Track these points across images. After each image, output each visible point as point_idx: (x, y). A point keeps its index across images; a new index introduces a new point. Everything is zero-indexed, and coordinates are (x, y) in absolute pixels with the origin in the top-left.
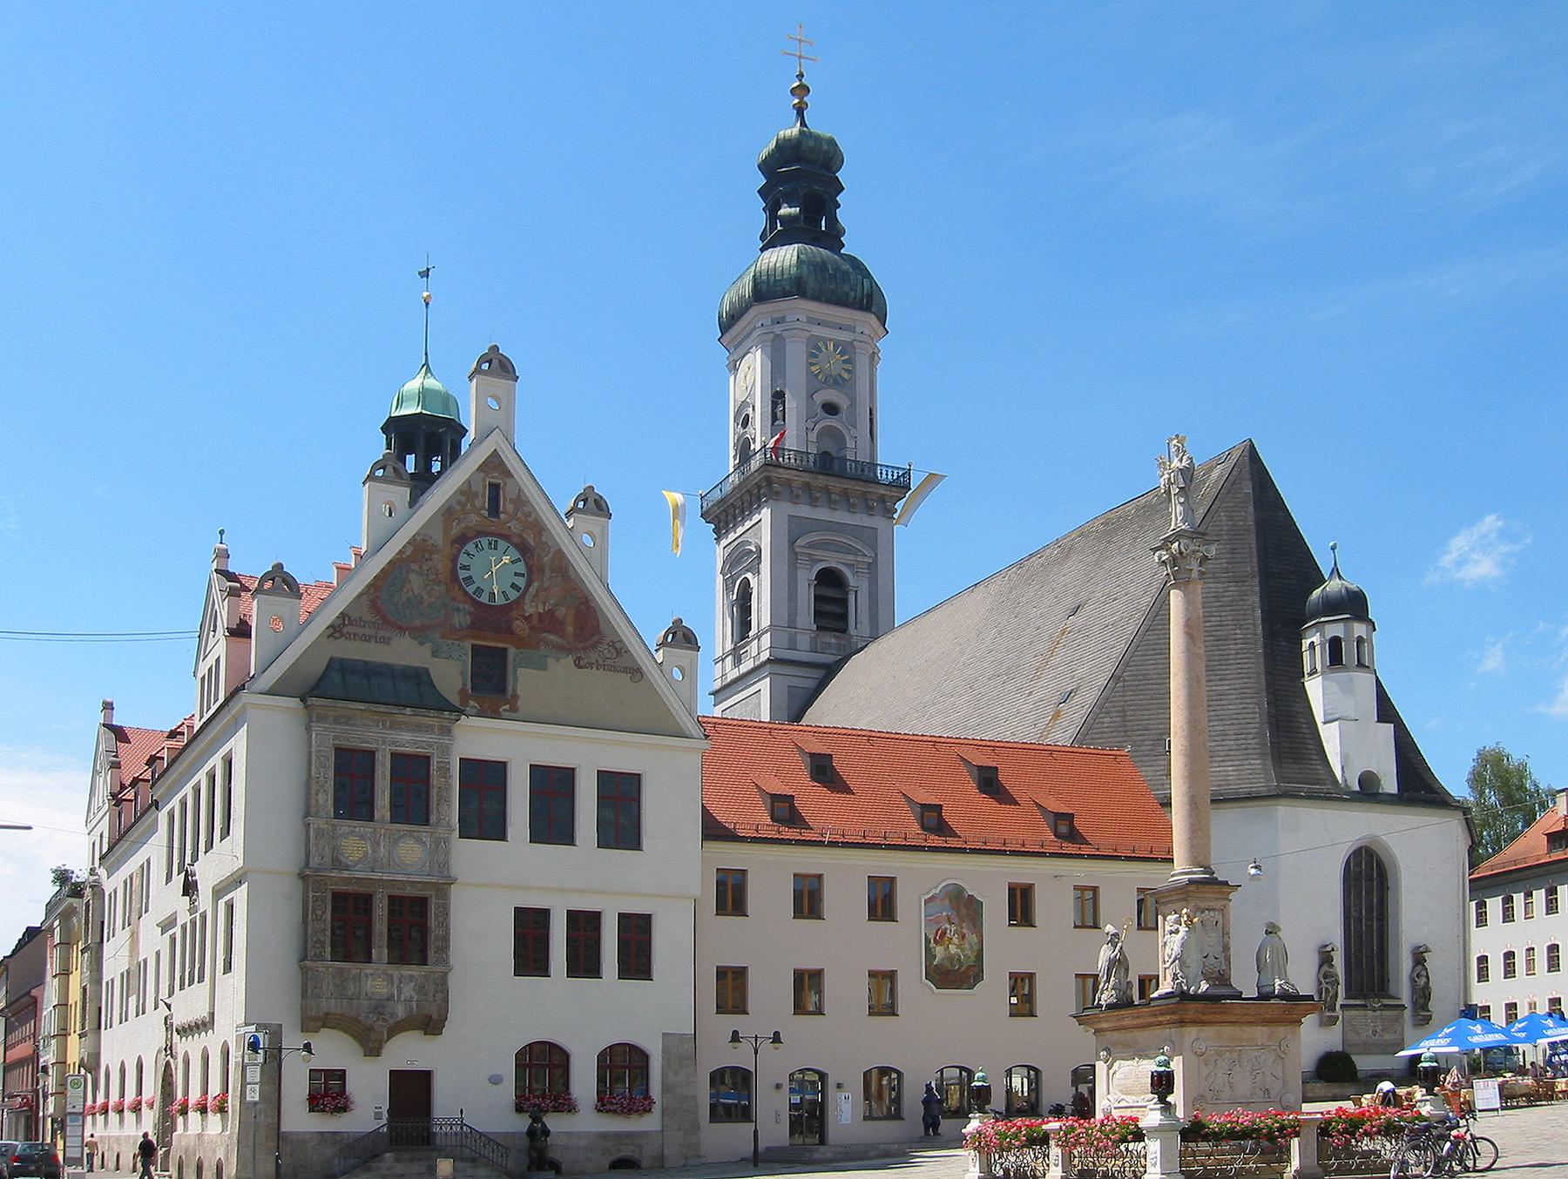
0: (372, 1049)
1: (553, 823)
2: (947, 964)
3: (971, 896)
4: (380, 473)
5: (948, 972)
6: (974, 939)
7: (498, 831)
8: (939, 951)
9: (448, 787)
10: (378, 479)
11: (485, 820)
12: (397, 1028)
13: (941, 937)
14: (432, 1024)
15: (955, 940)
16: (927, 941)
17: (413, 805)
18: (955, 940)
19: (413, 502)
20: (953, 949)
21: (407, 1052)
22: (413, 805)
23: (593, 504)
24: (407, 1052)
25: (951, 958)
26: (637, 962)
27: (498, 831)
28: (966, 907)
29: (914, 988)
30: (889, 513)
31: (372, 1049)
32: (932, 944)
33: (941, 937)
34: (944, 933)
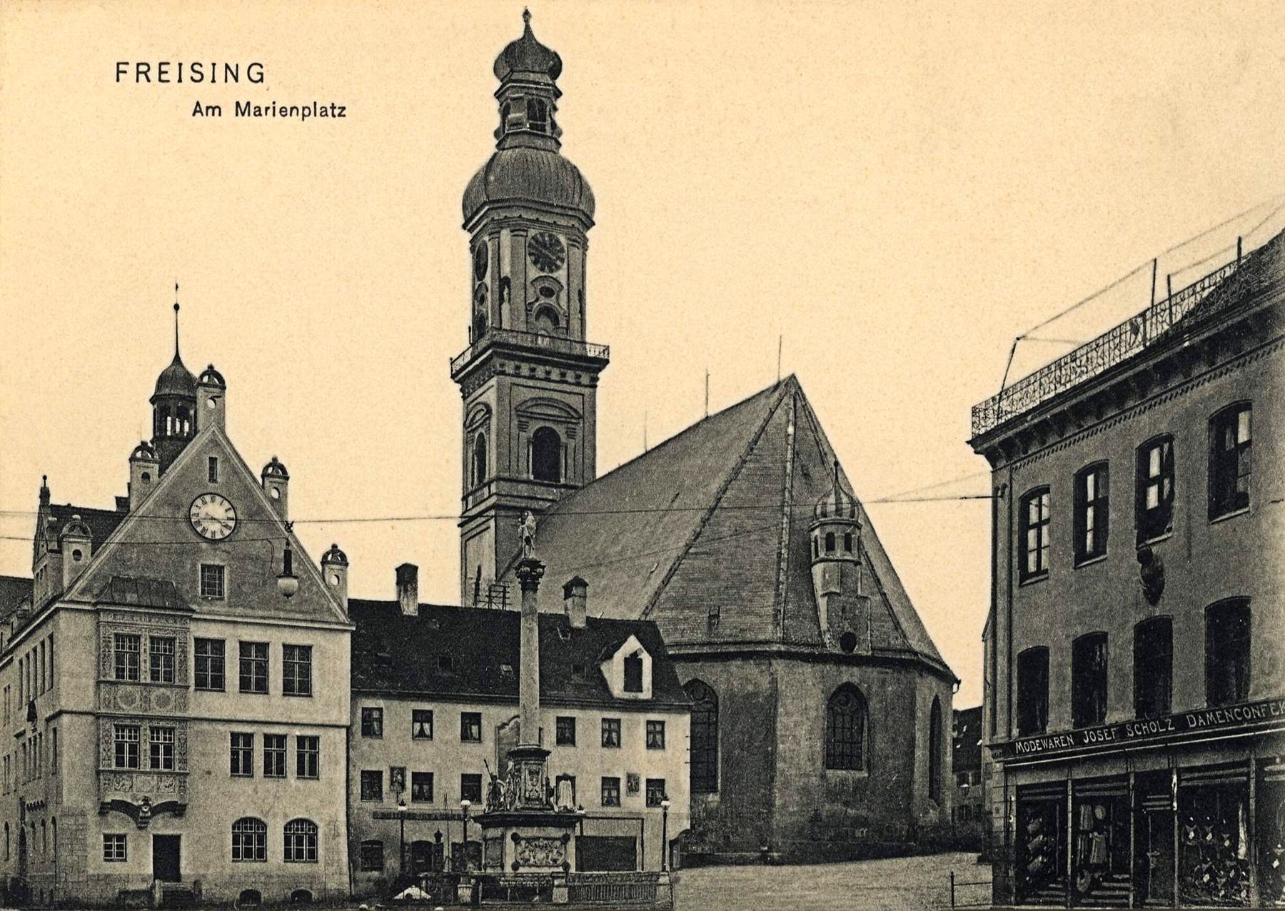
0: (142, 825)
1: (254, 682)
4: (139, 454)
7: (218, 684)
9: (184, 661)
10: (139, 460)
11: (212, 680)
12: (156, 811)
14: (177, 810)
17: (165, 672)
19: (162, 471)
21: (163, 826)
22: (165, 672)
23: (276, 471)
24: (163, 826)
26: (309, 768)
27: (218, 684)
31: (142, 825)
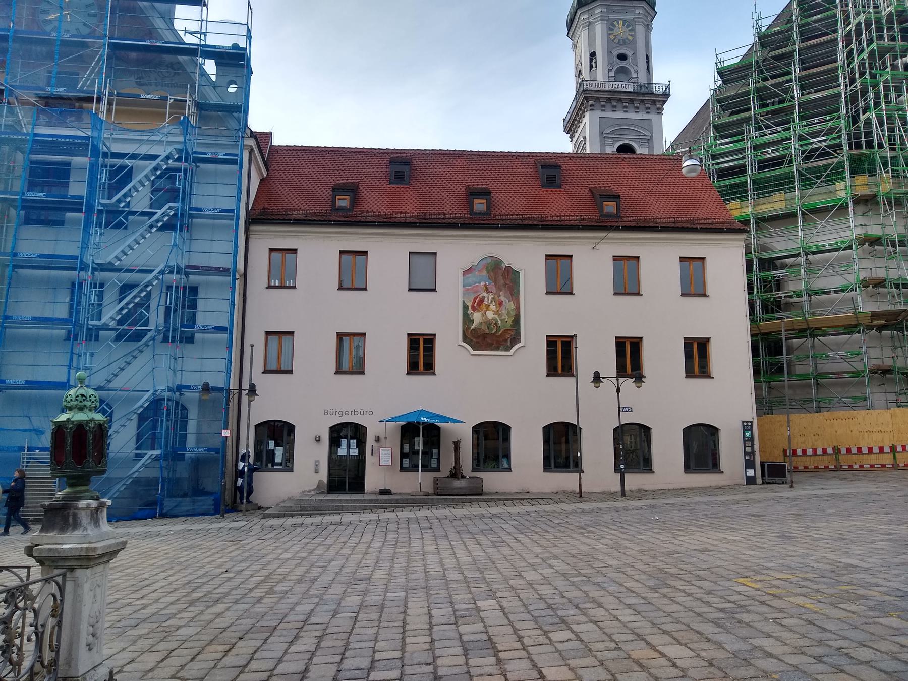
2: (484, 328)
3: (509, 269)
5: (484, 336)
6: (512, 306)
8: (477, 317)
13: (479, 304)
15: (493, 307)
16: (465, 307)
18: (493, 307)
20: (490, 315)
25: (488, 323)
28: (505, 278)
29: (450, 349)
30: (660, 111)
32: (470, 311)
33: (479, 304)
34: (482, 301)
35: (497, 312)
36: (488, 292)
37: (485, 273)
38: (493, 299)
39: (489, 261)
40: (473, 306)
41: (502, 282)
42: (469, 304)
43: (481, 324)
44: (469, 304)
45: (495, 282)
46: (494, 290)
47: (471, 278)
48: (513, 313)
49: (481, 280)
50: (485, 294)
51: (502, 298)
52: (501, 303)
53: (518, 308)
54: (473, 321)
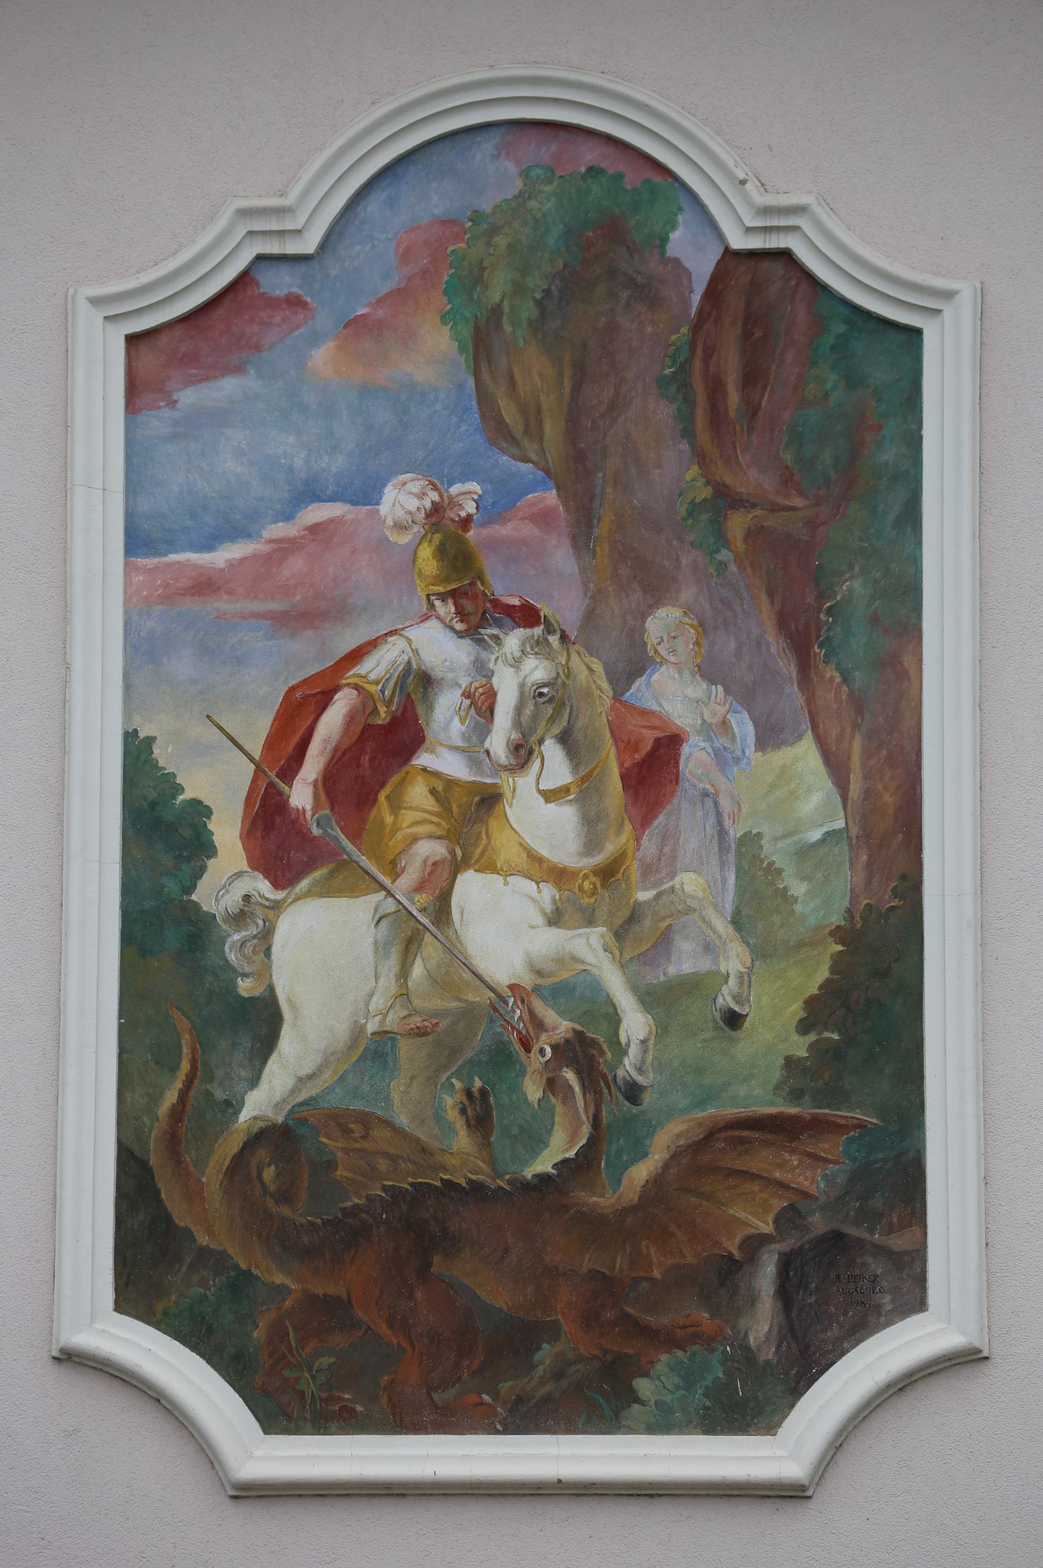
2: (420, 1107)
3: (764, 284)
6: (797, 793)
8: (322, 962)
13: (350, 779)
15: (541, 816)
16: (159, 828)
18: (541, 816)
20: (504, 929)
32: (229, 877)
33: (350, 779)
34: (389, 739)
35: (590, 892)
36: (478, 612)
37: (432, 357)
38: (550, 703)
39: (496, 179)
40: (269, 822)
41: (670, 472)
42: (218, 785)
43: (374, 1051)
44: (218, 785)
45: (578, 475)
46: (557, 576)
47: (248, 430)
48: (819, 901)
49: (378, 448)
50: (437, 644)
51: (674, 694)
52: (652, 769)
53: (890, 831)
54: (260, 1022)
